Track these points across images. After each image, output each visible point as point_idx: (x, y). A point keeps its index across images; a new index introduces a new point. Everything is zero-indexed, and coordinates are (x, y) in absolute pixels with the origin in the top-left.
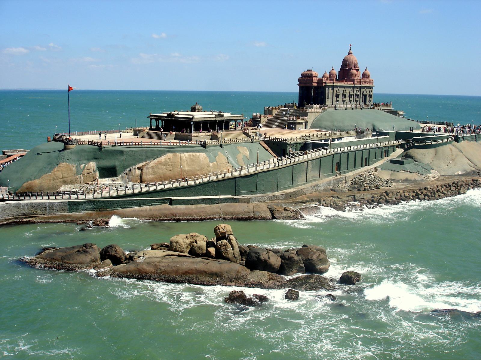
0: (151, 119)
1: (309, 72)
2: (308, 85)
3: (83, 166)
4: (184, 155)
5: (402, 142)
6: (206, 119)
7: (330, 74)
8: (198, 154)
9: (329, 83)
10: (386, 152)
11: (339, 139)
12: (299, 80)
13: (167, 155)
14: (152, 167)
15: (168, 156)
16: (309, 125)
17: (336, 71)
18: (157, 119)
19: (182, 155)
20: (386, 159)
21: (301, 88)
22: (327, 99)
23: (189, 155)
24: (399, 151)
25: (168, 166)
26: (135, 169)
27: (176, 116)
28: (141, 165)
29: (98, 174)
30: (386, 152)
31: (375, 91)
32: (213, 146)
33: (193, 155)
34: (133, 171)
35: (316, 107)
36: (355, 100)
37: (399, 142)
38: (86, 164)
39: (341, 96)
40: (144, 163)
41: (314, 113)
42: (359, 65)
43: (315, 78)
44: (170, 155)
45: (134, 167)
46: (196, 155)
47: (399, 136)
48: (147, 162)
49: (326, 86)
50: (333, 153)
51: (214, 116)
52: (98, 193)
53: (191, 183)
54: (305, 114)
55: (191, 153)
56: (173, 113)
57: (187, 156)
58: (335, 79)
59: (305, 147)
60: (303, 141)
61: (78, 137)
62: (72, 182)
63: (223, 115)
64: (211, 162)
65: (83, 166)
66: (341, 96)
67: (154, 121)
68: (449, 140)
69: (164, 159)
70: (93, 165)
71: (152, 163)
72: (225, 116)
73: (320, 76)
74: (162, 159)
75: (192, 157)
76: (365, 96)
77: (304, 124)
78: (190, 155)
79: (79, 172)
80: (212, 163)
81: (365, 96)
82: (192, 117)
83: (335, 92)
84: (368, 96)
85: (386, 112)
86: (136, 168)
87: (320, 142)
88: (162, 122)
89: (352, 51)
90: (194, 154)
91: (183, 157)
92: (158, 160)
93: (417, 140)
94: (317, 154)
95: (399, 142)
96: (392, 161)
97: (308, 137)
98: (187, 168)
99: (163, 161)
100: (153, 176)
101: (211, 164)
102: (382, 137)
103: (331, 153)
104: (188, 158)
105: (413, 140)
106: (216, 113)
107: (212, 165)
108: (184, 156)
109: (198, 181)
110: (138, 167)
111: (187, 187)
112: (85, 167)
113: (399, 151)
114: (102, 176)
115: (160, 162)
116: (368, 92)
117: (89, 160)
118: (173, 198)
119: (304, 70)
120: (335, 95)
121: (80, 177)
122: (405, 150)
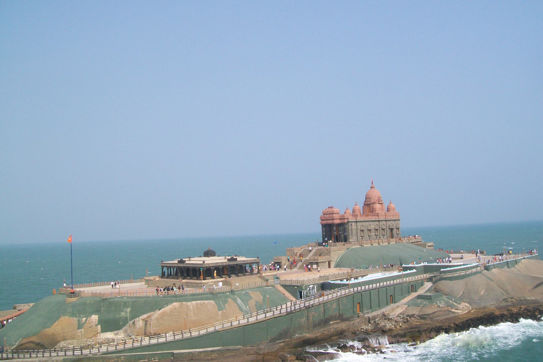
0: (163, 267)
1: (330, 210)
2: (330, 222)
3: (84, 319)
5: (431, 275)
7: (354, 211)
8: (206, 302)
9: (351, 219)
10: (413, 287)
11: (362, 276)
12: (321, 218)
14: (157, 319)
16: (333, 265)
17: (360, 206)
18: (169, 267)
19: (189, 303)
20: (414, 295)
21: (324, 226)
22: (350, 237)
23: (197, 304)
24: (428, 285)
26: (139, 321)
27: (187, 262)
28: (145, 316)
29: (99, 326)
30: (413, 287)
31: (402, 225)
32: (223, 293)
33: (200, 304)
35: (340, 245)
36: (381, 234)
37: (428, 276)
38: (87, 317)
39: (366, 232)
40: (149, 314)
41: (338, 251)
42: (382, 199)
43: (337, 215)
44: (176, 304)
47: (426, 269)
49: (348, 222)
50: (353, 293)
51: (226, 261)
52: (96, 348)
53: (195, 334)
54: (329, 253)
55: (199, 302)
56: (184, 259)
58: (359, 215)
59: (324, 287)
60: (322, 282)
61: (82, 289)
62: (73, 338)
63: (236, 259)
64: (219, 310)
65: (84, 319)
66: (366, 232)
67: (165, 269)
68: (479, 269)
70: (95, 318)
71: (158, 313)
72: (238, 260)
73: (342, 213)
76: (392, 230)
77: (327, 263)
79: (80, 326)
81: (392, 230)
82: (202, 262)
83: (359, 227)
84: (395, 230)
85: (416, 245)
87: (339, 282)
88: (168, 269)
89: (374, 185)
91: (190, 306)
92: (163, 310)
93: (444, 272)
94: (335, 295)
95: (428, 276)
96: (419, 297)
97: (327, 277)
98: (193, 318)
99: (168, 311)
101: (220, 312)
102: (408, 272)
103: (351, 293)
105: (441, 272)
106: (229, 258)
109: (203, 332)
111: (191, 339)
112: (86, 320)
113: (428, 285)
114: (104, 330)
116: (395, 226)
117: (91, 314)
118: (175, 351)
119: (324, 208)
120: (359, 231)
121: (81, 332)
122: (434, 283)
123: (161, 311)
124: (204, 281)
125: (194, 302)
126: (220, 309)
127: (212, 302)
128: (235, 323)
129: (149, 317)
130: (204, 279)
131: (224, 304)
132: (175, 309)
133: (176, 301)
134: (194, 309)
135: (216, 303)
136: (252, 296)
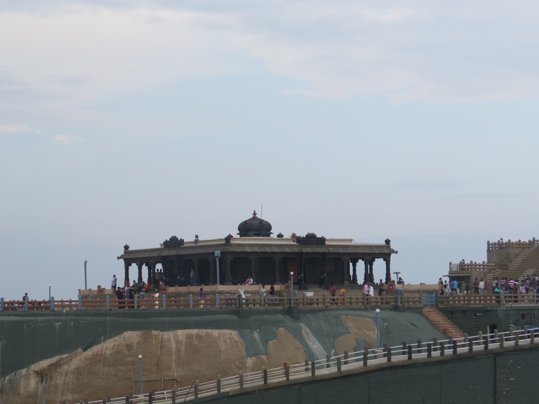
4: (174, 336)
6: (267, 250)
8: (215, 332)
13: (122, 336)
14: (78, 371)
15: (124, 338)
19: (167, 335)
23: (189, 337)
25: (124, 368)
28: (44, 364)
33: (199, 337)
34: (23, 383)
44: (132, 336)
45: (24, 371)
46: (207, 335)
48: (65, 356)
55: (194, 331)
57: (181, 338)
64: (249, 354)
67: (134, 268)
69: (113, 347)
71: (79, 358)
74: (107, 346)
75: (195, 342)
78: (192, 335)
80: (254, 358)
86: (29, 374)
90: (203, 332)
91: (169, 340)
92: (96, 349)
98: (176, 373)
99: (108, 352)
100: (76, 396)
101: (250, 361)
104: (184, 343)
107: (254, 363)
108: (172, 338)
110: (36, 369)
115: (101, 355)
123: (89, 353)
124: (221, 288)
125: (182, 333)
126: (252, 351)
127: (234, 334)
128: (277, 377)
129: (56, 366)
130: (222, 283)
131: (265, 341)
132: (129, 346)
133: (133, 328)
134: (178, 351)
135: (242, 336)
136: (349, 324)
